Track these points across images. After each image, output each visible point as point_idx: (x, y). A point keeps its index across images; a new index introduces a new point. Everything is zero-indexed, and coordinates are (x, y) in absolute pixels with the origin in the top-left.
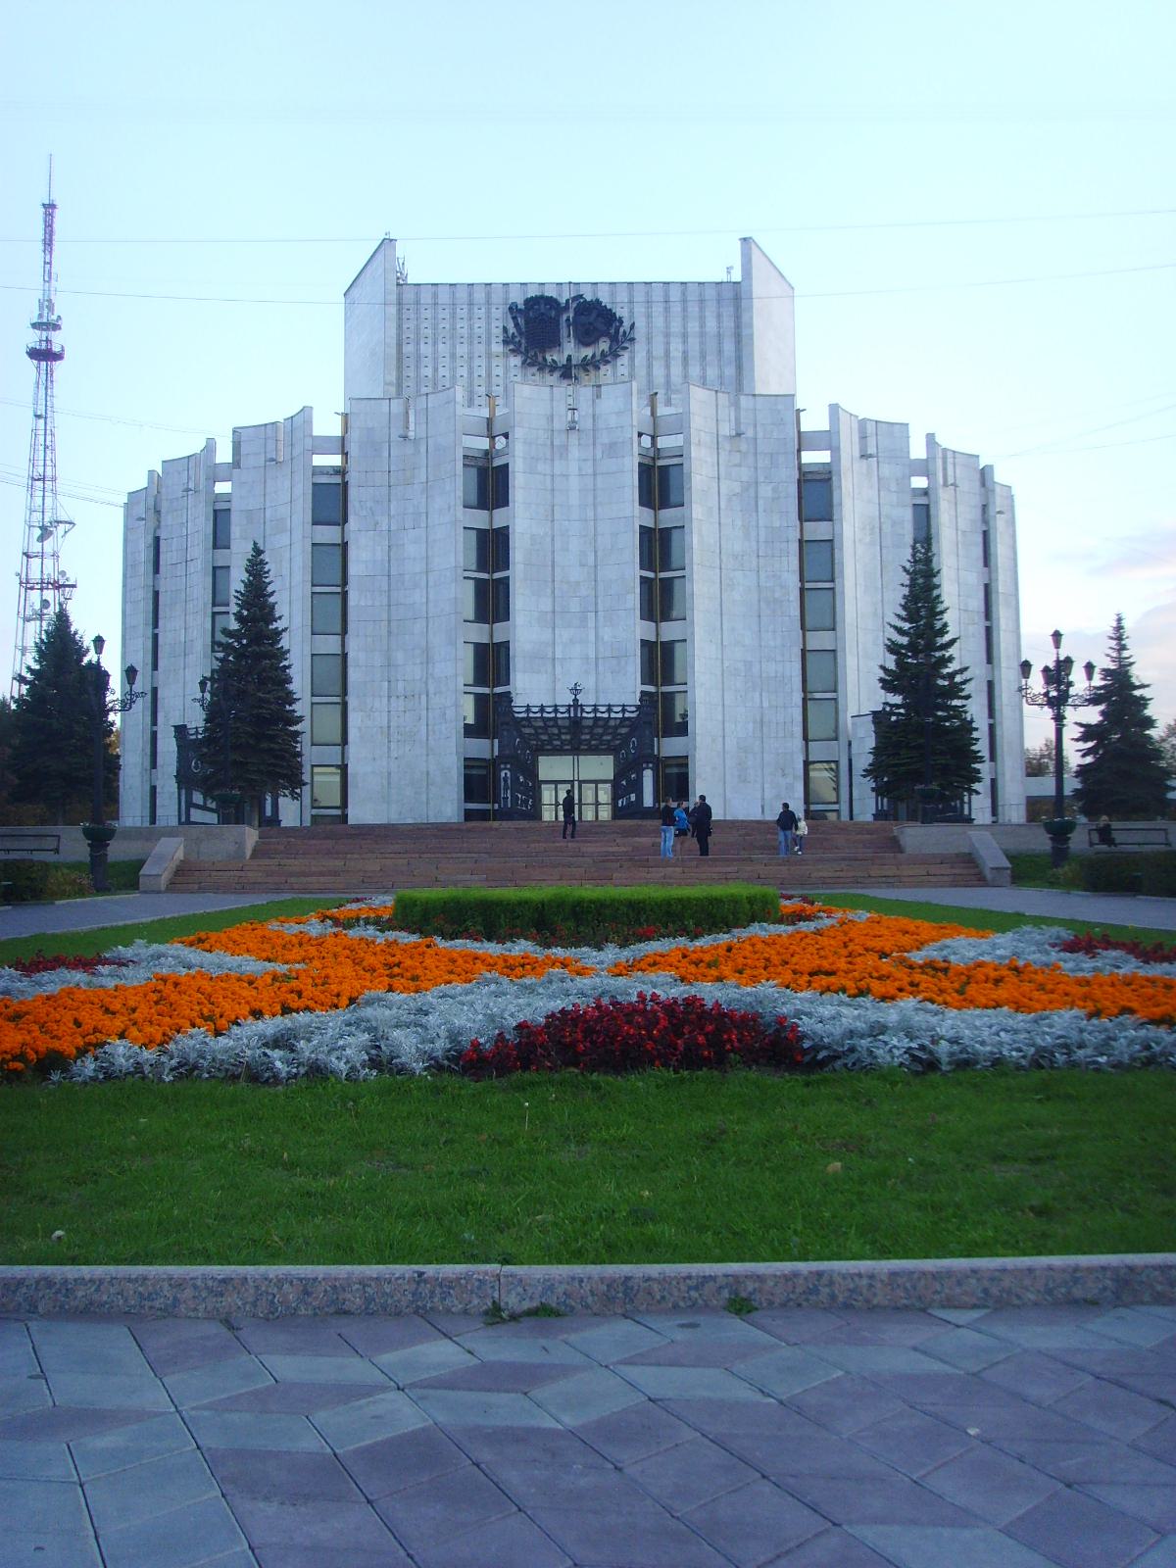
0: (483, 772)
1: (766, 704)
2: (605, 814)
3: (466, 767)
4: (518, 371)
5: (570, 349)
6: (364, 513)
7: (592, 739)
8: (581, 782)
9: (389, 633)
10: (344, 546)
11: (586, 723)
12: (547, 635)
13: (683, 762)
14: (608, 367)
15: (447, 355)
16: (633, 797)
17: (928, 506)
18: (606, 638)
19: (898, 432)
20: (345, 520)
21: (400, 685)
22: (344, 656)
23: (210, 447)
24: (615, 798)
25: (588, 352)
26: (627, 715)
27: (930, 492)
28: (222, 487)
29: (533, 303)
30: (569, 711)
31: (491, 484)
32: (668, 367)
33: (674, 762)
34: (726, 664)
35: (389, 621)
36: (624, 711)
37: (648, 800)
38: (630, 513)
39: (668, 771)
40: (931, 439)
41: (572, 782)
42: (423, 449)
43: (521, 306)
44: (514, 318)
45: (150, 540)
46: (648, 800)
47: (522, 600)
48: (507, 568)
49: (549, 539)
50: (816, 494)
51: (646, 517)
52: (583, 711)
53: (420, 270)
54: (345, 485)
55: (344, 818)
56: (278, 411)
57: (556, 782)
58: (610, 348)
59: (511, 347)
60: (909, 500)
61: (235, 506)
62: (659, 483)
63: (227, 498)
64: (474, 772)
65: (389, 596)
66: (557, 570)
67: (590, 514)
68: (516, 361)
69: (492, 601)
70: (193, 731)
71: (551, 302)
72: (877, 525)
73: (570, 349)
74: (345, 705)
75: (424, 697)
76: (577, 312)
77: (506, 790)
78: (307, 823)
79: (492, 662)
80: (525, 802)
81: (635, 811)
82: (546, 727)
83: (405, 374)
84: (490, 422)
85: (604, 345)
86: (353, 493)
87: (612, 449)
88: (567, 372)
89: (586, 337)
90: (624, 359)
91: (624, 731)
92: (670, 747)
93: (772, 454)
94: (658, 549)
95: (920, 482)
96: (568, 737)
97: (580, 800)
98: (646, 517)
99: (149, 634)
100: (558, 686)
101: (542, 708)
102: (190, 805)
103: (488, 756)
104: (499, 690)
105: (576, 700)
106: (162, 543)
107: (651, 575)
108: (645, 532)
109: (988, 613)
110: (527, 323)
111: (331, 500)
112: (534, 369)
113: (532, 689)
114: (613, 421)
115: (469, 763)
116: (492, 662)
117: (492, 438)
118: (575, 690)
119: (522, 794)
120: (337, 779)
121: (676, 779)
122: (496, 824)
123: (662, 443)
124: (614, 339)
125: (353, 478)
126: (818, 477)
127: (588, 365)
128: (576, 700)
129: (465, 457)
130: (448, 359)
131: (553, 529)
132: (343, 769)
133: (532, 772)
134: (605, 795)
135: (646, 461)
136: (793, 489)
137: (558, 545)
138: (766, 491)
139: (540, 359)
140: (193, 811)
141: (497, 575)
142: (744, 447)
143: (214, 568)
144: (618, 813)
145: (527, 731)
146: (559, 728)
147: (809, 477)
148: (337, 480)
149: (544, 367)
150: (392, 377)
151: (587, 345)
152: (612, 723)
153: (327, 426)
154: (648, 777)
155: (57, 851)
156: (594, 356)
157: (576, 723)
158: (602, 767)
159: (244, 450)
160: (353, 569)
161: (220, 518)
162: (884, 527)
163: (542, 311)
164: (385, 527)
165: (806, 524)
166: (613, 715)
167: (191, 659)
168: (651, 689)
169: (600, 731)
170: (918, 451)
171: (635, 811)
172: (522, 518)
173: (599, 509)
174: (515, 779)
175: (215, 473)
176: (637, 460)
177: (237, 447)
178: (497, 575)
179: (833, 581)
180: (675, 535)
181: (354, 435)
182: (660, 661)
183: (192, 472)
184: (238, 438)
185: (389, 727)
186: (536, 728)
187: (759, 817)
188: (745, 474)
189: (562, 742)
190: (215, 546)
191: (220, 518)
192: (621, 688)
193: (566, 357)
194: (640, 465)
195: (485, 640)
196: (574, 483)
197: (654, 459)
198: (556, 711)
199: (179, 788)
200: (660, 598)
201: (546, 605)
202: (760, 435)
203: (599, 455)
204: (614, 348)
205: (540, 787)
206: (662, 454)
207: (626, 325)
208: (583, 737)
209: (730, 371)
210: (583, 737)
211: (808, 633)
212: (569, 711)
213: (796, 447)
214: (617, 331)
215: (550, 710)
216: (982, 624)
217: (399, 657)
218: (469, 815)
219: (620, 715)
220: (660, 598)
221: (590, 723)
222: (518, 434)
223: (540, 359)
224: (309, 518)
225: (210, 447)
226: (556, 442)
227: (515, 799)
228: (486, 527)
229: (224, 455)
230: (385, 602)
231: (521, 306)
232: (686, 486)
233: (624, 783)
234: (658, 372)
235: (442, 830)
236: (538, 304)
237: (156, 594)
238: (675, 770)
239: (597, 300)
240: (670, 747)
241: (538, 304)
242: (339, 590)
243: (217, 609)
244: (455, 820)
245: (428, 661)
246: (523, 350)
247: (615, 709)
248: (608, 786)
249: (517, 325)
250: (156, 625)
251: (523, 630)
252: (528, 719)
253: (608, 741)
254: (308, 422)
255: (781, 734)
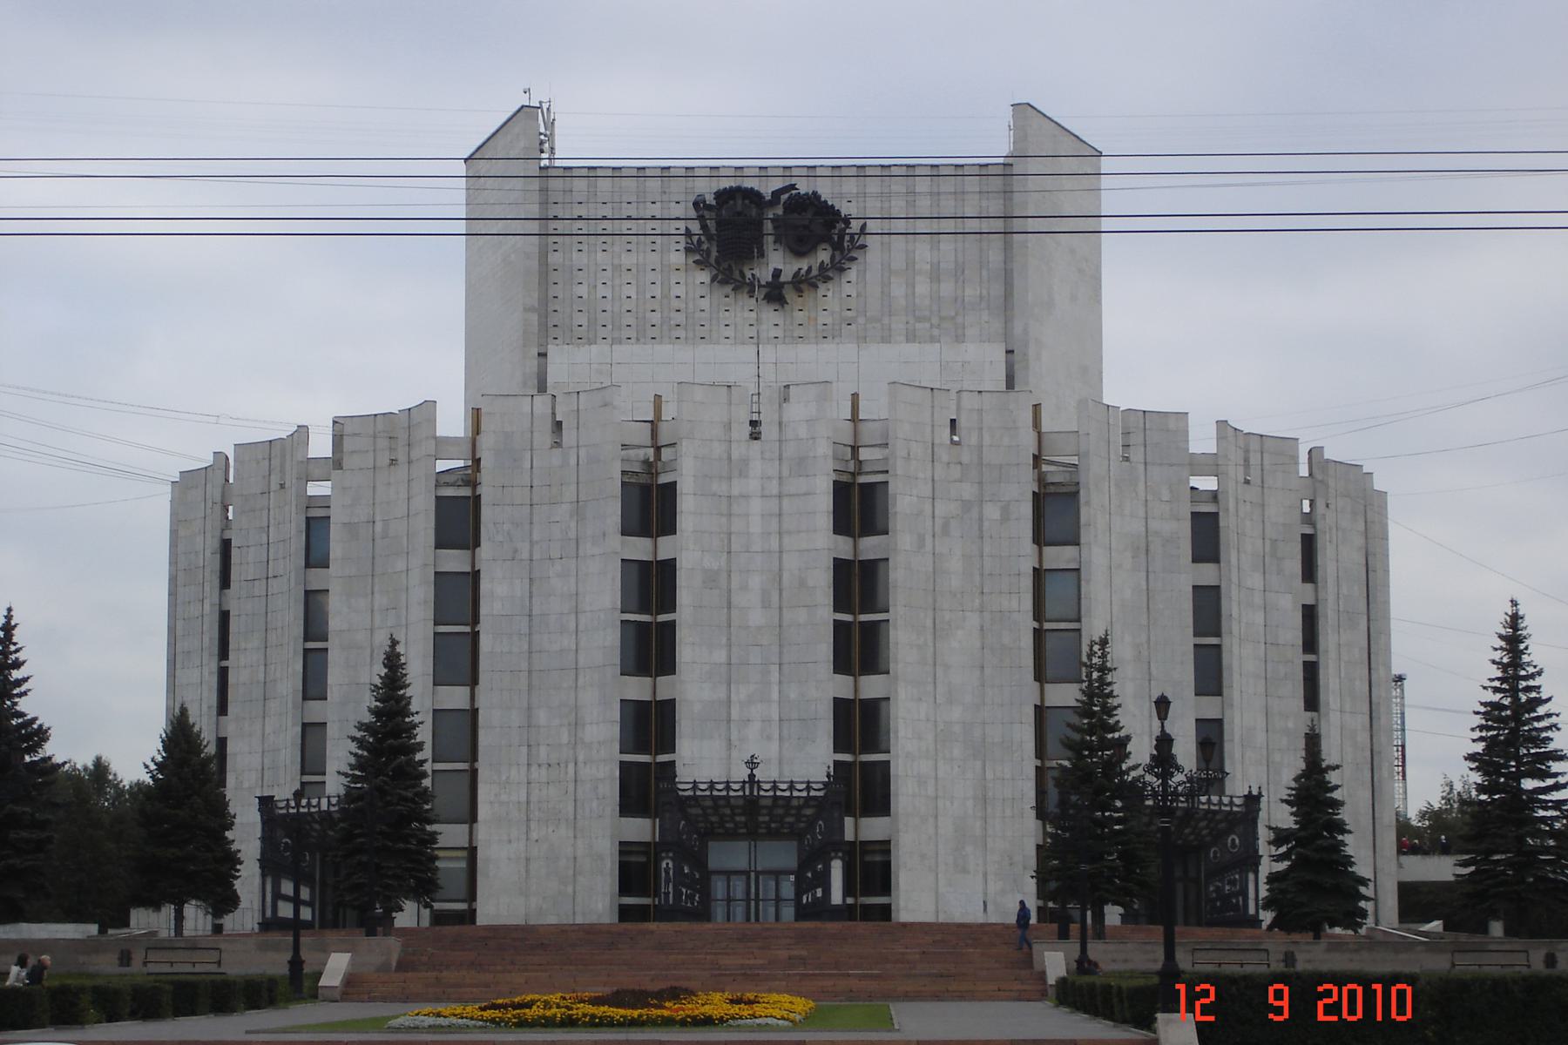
0: (642, 859)
1: (989, 775)
2: (788, 912)
3: (621, 853)
4: (704, 290)
5: (776, 261)
6: (500, 538)
7: (771, 821)
8: (758, 873)
9: (530, 687)
10: (476, 575)
11: (763, 802)
12: (721, 693)
13: (885, 847)
14: (830, 285)
15: (609, 268)
16: (819, 893)
17: (1215, 515)
18: (792, 696)
19: (1170, 425)
20: (477, 544)
21: (543, 750)
22: (474, 712)
23: (302, 432)
24: (798, 895)
25: (803, 264)
26: (813, 793)
27: (1220, 497)
28: (316, 489)
29: (724, 196)
30: (743, 788)
31: (651, 504)
32: (911, 285)
33: (877, 847)
34: (941, 726)
35: (530, 672)
36: (808, 788)
37: (837, 897)
38: (818, 544)
39: (868, 858)
40: (1222, 424)
41: (747, 873)
42: (573, 461)
43: (710, 199)
44: (701, 218)
45: (213, 544)
46: (837, 897)
47: (687, 651)
48: (673, 609)
49: (724, 575)
50: (1055, 509)
51: (843, 547)
52: (759, 788)
53: (574, 145)
54: (477, 499)
55: (469, 916)
56: (394, 401)
57: (728, 874)
58: (833, 258)
59: (698, 257)
60: (1186, 510)
61: (337, 516)
62: (859, 505)
63: (324, 502)
64: (633, 859)
65: (530, 643)
66: (734, 612)
67: (774, 544)
68: (704, 276)
69: (651, 649)
70: (283, 804)
71: (752, 196)
72: (1143, 545)
73: (776, 261)
74: (474, 773)
75: (571, 767)
76: (789, 207)
77: (668, 881)
78: (426, 923)
79: (650, 726)
80: (690, 897)
81: (820, 911)
82: (716, 807)
83: (551, 294)
84: (654, 424)
85: (824, 255)
86: (486, 513)
87: (802, 465)
88: (775, 294)
89: (800, 246)
90: (852, 274)
91: (809, 812)
92: (873, 828)
93: (1001, 466)
94: (858, 585)
95: (1207, 483)
96: (743, 819)
97: (757, 894)
98: (843, 547)
99: (214, 666)
100: (735, 753)
101: (712, 785)
102: (277, 896)
103: (648, 839)
104: (662, 758)
105: (752, 776)
106: (234, 552)
107: (847, 618)
108: (841, 568)
109: (1310, 642)
110: (719, 224)
111: (459, 520)
112: (728, 289)
113: (700, 760)
114: (803, 432)
115: (625, 848)
116: (650, 726)
117: (658, 449)
118: (752, 763)
119: (688, 887)
120: (463, 865)
121: (874, 871)
122: (652, 926)
123: (864, 454)
124: (837, 246)
125: (485, 491)
126: (1064, 490)
127: (803, 283)
128: (752, 776)
129: (623, 473)
130: (609, 273)
131: (729, 561)
132: (472, 851)
133: (700, 861)
134: (788, 889)
135: (845, 478)
136: (1027, 509)
137: (735, 584)
138: (992, 512)
139: (737, 275)
140: (281, 904)
141: (662, 618)
142: (966, 458)
143: (307, 592)
144: (802, 913)
145: (694, 811)
146: (733, 808)
147: (1052, 489)
148: (465, 492)
149: (744, 286)
150: (533, 299)
151: (799, 254)
152: (795, 803)
153: (452, 422)
154: (837, 870)
155: (219, 963)
156: (810, 269)
157: (751, 804)
158: (782, 855)
159: (348, 444)
160: (487, 610)
161: (315, 527)
162: (1152, 547)
163: (739, 208)
164: (525, 555)
165: (1047, 550)
166: (796, 794)
167: (273, 705)
168: (847, 757)
169: (780, 811)
170: (1202, 441)
171: (820, 911)
172: (689, 548)
173: (786, 540)
174: (678, 870)
175: (310, 470)
176: (834, 477)
177: (338, 441)
178: (662, 618)
179: (1079, 620)
180: (881, 565)
181: (486, 443)
182: (859, 725)
183: (276, 462)
184: (341, 430)
185: (528, 803)
186: (704, 808)
187: (979, 918)
188: (968, 491)
189: (736, 824)
190: (308, 565)
191: (315, 527)
192: (808, 760)
193: (771, 270)
194: (835, 482)
195: (647, 697)
196: (756, 506)
197: (853, 474)
198: (728, 788)
199: (264, 876)
200: (859, 648)
201: (720, 656)
202: (987, 440)
203: (785, 473)
204: (838, 258)
205: (709, 879)
206: (866, 468)
207: (855, 226)
208: (761, 819)
209: (997, 290)
210: (761, 819)
211: (1048, 687)
212: (743, 788)
213: (1033, 450)
214: (841, 238)
215: (720, 787)
216: (1299, 658)
217: (542, 717)
218: (625, 913)
219: (804, 794)
220: (859, 648)
221: (769, 802)
222: (686, 447)
223: (737, 275)
224: (433, 544)
225: (302, 432)
226: (735, 455)
227: (678, 894)
228: (650, 558)
229: (320, 446)
230: (526, 647)
231: (710, 199)
232: (891, 511)
233: (810, 874)
234: (898, 290)
235: (590, 933)
236: (734, 198)
237: (224, 617)
238: (878, 858)
239: (815, 193)
240: (873, 828)
241: (734, 198)
242: (467, 629)
243: (311, 645)
244: (607, 921)
245: (577, 725)
246: (712, 260)
247: (799, 787)
248: (792, 878)
249: (704, 227)
250: (224, 653)
251: (692, 685)
252: (695, 798)
253: (791, 825)
254: (432, 421)
255: (1008, 812)
